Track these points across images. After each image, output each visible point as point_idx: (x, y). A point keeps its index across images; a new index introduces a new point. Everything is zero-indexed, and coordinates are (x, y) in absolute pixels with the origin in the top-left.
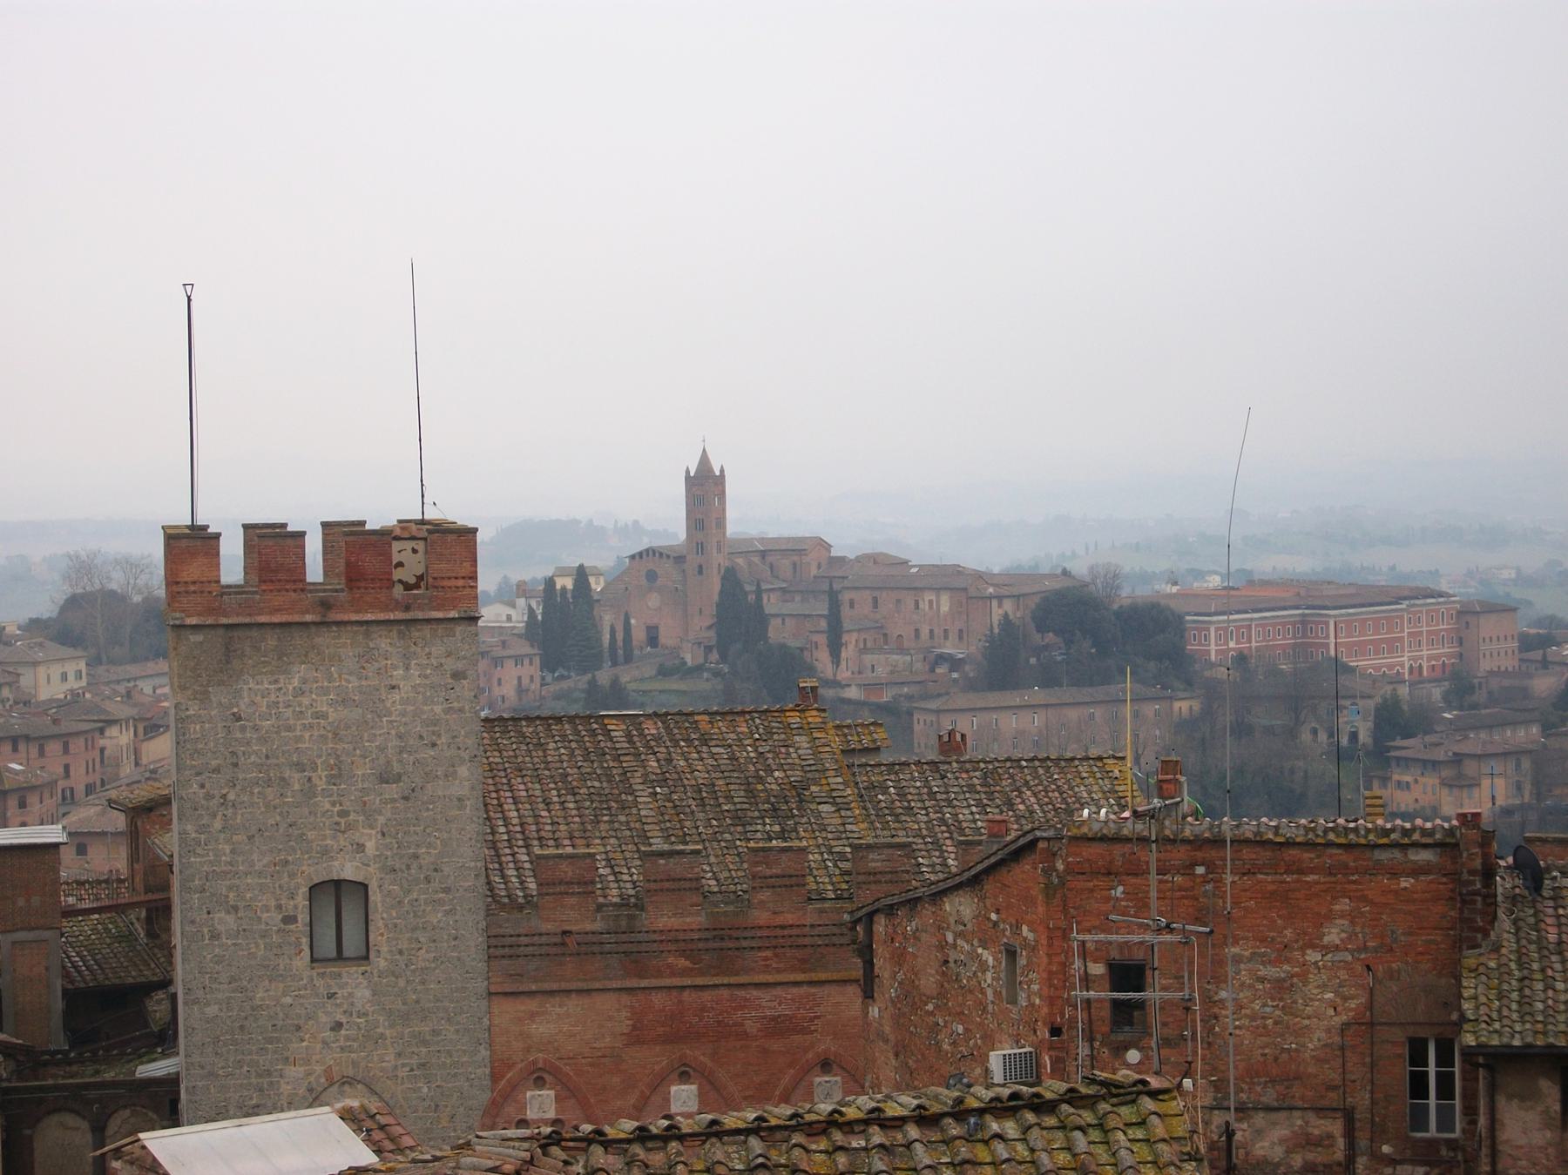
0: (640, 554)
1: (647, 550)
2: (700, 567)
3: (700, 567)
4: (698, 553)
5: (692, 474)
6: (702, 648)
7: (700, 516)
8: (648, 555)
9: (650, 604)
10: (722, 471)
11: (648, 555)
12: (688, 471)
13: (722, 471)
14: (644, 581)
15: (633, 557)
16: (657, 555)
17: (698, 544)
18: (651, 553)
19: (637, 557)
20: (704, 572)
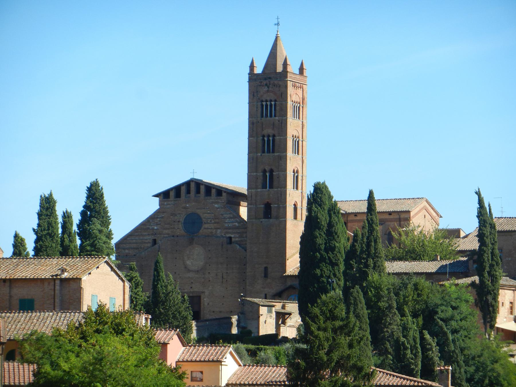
0: (177, 189)
1: (188, 184)
2: (268, 207)
3: (268, 207)
4: (264, 187)
5: (259, 70)
6: (274, 315)
7: (269, 131)
8: (188, 192)
9: (188, 263)
10: (301, 70)
11: (188, 192)
12: (252, 67)
13: (301, 70)
14: (180, 230)
15: (164, 196)
16: (202, 188)
17: (265, 171)
18: (193, 186)
19: (172, 194)
20: (274, 213)
